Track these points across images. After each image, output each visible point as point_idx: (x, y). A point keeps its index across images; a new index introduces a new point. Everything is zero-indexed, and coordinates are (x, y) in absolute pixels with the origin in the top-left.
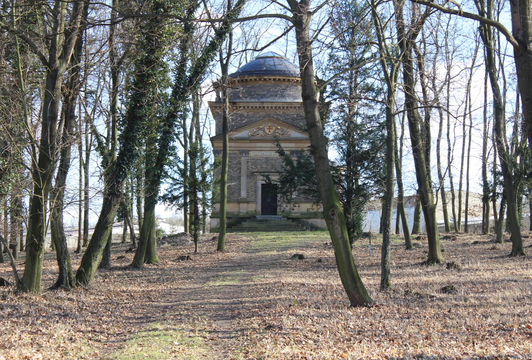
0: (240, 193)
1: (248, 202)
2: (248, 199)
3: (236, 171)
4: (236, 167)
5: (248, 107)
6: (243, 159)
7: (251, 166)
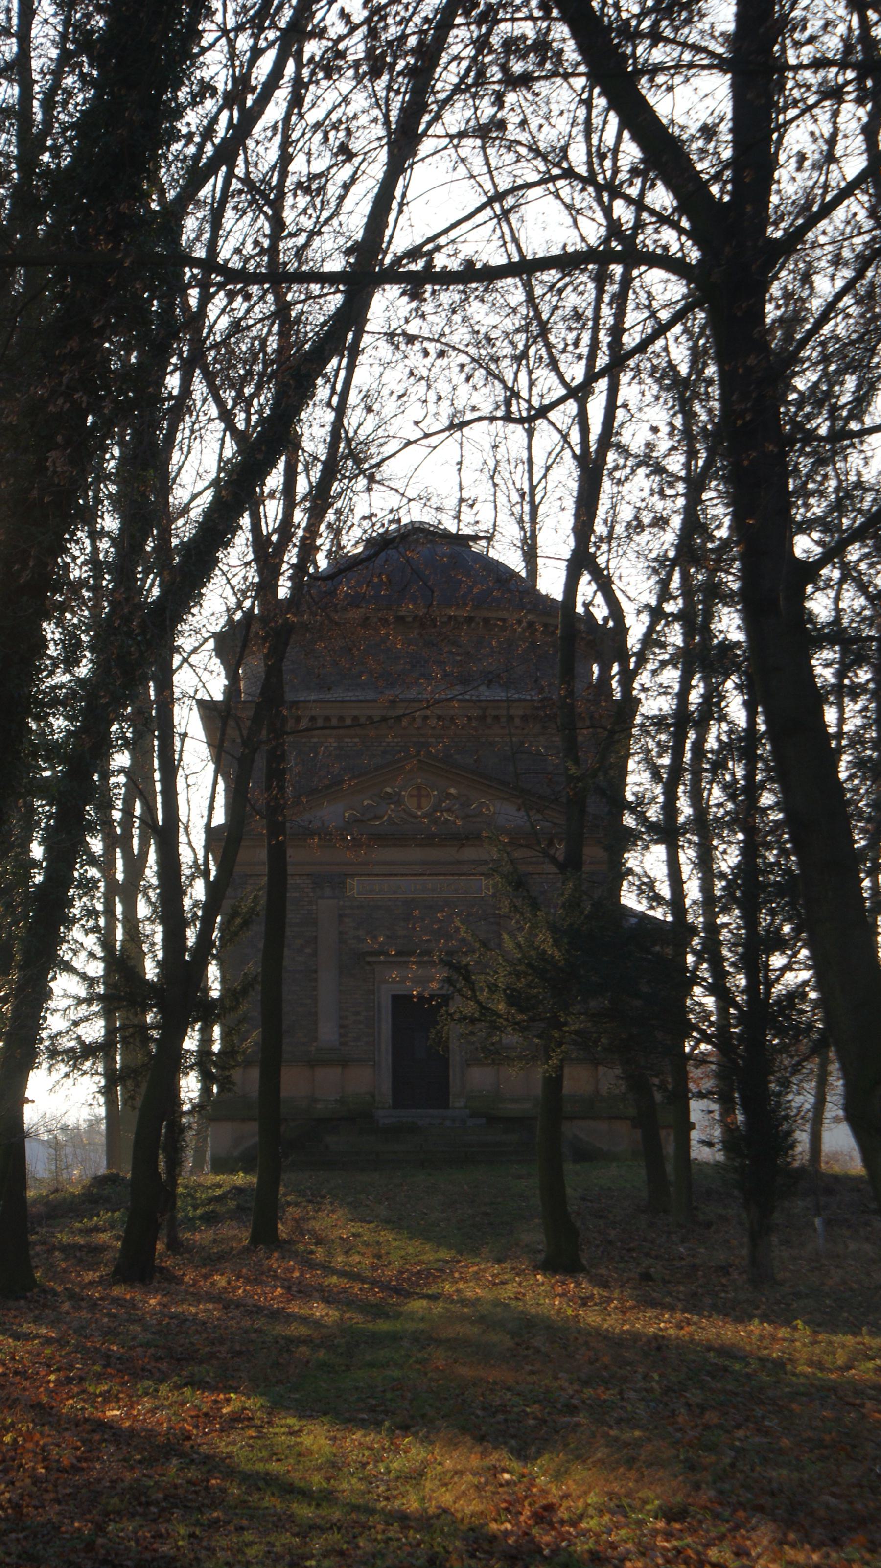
1: (344, 1063)
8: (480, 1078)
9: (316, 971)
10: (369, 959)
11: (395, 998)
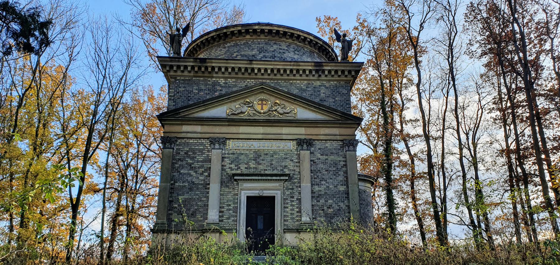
0: (207, 214)
2: (222, 224)
3: (202, 174)
4: (202, 167)
5: (226, 69)
6: (215, 154)
7: (228, 166)
8: (291, 239)
9: (209, 184)
10: (235, 178)
11: (248, 198)
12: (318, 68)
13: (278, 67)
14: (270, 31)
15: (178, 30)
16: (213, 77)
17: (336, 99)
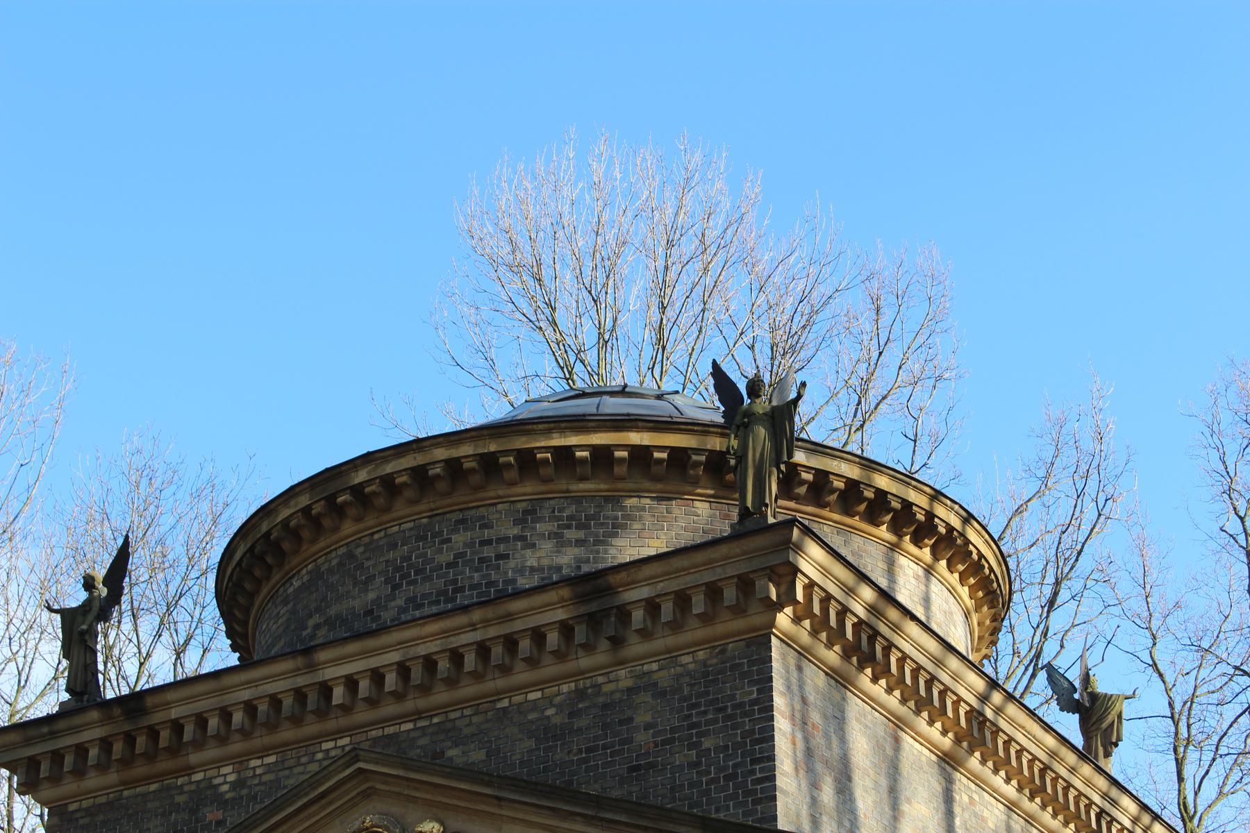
12: (593, 607)
13: (422, 650)
14: (419, 473)
15: (89, 584)
16: (189, 770)
17: (707, 743)
